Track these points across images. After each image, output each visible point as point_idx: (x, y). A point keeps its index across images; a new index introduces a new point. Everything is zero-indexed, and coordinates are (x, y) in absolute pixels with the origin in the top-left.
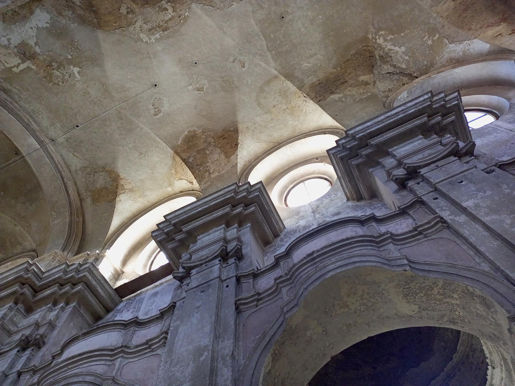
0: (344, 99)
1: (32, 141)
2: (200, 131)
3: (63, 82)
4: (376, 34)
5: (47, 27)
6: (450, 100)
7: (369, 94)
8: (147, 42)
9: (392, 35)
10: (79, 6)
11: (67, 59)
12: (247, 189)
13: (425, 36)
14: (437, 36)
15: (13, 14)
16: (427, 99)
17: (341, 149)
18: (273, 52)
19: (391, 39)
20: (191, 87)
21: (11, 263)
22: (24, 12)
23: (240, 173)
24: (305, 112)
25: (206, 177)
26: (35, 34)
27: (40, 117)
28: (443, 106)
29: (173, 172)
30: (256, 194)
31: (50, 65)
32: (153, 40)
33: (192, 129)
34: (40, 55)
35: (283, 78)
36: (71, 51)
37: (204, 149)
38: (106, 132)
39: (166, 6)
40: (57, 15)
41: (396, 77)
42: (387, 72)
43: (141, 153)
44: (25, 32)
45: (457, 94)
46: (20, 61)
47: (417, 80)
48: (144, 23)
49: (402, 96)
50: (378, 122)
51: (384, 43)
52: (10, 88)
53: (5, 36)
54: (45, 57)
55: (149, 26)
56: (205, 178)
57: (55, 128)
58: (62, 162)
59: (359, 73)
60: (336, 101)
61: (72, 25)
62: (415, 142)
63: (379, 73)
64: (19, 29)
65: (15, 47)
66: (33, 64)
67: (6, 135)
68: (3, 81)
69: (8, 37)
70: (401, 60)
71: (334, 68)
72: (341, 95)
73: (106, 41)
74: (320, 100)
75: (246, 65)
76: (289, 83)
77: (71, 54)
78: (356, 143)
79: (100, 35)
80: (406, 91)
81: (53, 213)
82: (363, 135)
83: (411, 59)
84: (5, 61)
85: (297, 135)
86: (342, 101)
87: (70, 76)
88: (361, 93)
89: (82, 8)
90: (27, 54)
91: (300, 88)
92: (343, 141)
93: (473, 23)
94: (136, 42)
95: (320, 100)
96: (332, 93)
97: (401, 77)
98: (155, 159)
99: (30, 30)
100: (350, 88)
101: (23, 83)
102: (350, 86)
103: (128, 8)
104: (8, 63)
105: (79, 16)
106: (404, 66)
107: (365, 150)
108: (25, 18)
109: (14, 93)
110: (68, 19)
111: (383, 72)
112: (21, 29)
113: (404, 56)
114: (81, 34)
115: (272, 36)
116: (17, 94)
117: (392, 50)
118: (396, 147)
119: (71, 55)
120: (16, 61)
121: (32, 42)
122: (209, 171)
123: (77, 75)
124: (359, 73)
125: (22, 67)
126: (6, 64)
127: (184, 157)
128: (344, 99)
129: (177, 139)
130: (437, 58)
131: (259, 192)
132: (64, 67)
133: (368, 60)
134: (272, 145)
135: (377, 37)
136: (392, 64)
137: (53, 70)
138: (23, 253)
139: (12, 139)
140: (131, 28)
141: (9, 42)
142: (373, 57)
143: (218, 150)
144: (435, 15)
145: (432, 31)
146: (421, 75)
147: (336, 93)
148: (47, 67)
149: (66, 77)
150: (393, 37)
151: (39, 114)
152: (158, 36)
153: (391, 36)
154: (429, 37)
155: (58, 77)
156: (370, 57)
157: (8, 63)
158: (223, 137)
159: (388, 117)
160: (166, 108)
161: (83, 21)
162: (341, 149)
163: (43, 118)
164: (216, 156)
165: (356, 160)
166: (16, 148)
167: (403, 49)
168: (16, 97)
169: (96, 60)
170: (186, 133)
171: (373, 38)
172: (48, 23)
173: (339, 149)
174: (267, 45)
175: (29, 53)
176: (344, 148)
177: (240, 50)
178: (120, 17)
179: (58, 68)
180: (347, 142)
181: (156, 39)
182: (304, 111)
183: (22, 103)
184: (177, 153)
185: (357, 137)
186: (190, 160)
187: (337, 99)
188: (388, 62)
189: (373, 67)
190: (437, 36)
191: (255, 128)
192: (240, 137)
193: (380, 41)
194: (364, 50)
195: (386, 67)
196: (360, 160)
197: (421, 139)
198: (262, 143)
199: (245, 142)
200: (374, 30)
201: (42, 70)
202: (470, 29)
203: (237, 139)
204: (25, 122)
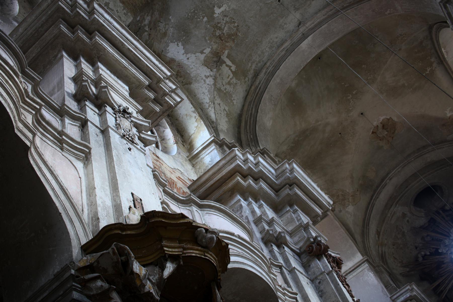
1: (304, 45)
3: (234, 22)
5: (183, 45)
10: (152, 17)
11: (208, 22)
15: (181, 77)
21: (443, 49)
26: (193, 55)
27: (276, 40)
31: (220, 37)
34: (212, 48)
36: (199, 18)
40: (167, 38)
44: (193, 64)
46: (224, 65)
52: (252, 72)
53: (205, 81)
54: (212, 43)
57: (285, 24)
58: (323, 12)
61: (172, 21)
64: (193, 70)
65: (211, 70)
66: (224, 53)
67: (302, 70)
68: (247, 79)
69: (204, 78)
77: (201, 18)
81: (388, 12)
84: (228, 78)
89: (153, 13)
90: (215, 59)
99: (190, 60)
101: (244, 60)
104: (229, 76)
108: (180, 65)
109: (256, 67)
110: (167, 26)
112: (192, 68)
116: (257, 64)
119: (203, 17)
120: (225, 69)
121: (202, 57)
123: (222, 9)
125: (229, 62)
126: (231, 77)
132: (218, 23)
137: (224, 34)
138: (432, 39)
139: (305, 64)
141: (209, 76)
148: (222, 40)
149: (228, 19)
151: (273, 41)
155: (229, 28)
157: (229, 76)
163: (277, 38)
166: (313, 59)
168: (259, 65)
172: (178, 44)
175: (213, 58)
179: (220, 29)
183: (265, 59)
201: (227, 44)
204: (285, 54)
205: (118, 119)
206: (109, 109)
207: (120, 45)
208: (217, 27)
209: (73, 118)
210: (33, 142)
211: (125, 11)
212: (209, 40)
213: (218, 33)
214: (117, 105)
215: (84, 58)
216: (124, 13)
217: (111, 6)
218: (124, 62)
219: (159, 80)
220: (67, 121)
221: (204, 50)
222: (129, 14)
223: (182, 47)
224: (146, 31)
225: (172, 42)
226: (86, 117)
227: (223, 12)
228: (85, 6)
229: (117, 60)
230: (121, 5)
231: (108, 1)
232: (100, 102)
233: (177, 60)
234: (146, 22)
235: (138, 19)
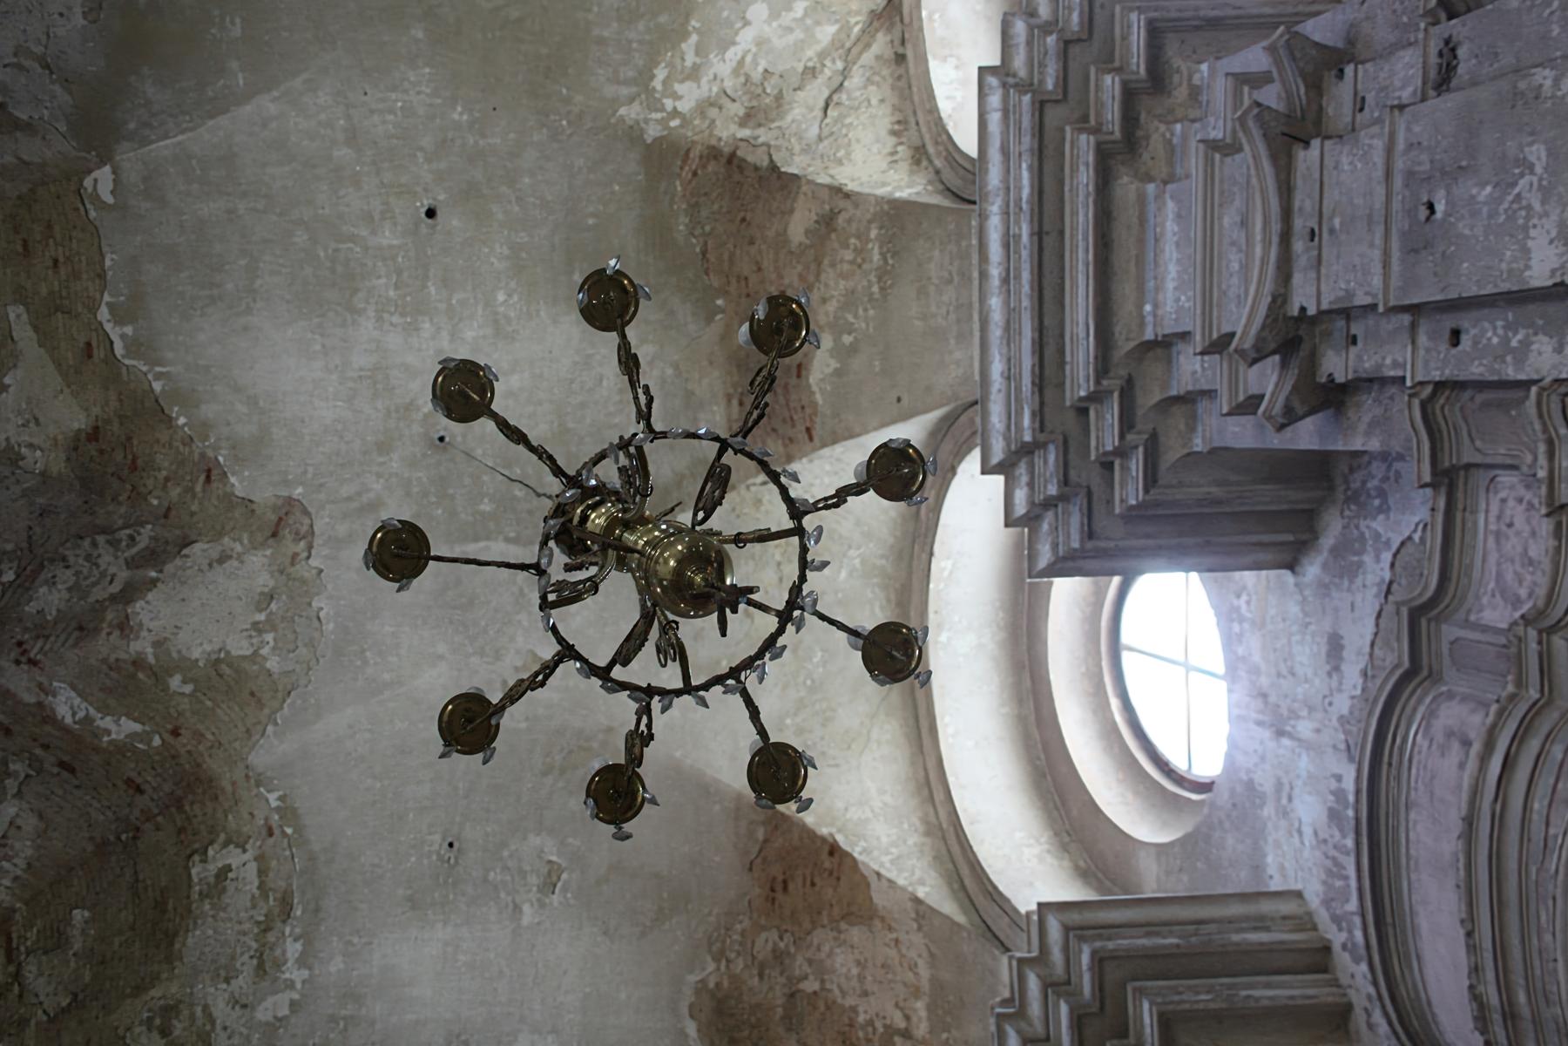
0: (847, 339)
50: (1007, 327)
59: (771, 233)
60: (838, 373)
63: (806, 150)
71: (709, 319)
74: (808, 430)
86: (853, 349)
88: (852, 262)
92: (1020, 496)
95: (808, 430)
102: (810, 288)
106: (827, 33)
115: (486, 507)
124: (771, 233)
128: (847, 339)
133: (737, 177)
174: (508, 540)
176: (1049, 504)
177: (481, 653)
180: (1031, 485)
187: (834, 364)
195: (796, 112)
198: (875, 735)
200: (636, 106)
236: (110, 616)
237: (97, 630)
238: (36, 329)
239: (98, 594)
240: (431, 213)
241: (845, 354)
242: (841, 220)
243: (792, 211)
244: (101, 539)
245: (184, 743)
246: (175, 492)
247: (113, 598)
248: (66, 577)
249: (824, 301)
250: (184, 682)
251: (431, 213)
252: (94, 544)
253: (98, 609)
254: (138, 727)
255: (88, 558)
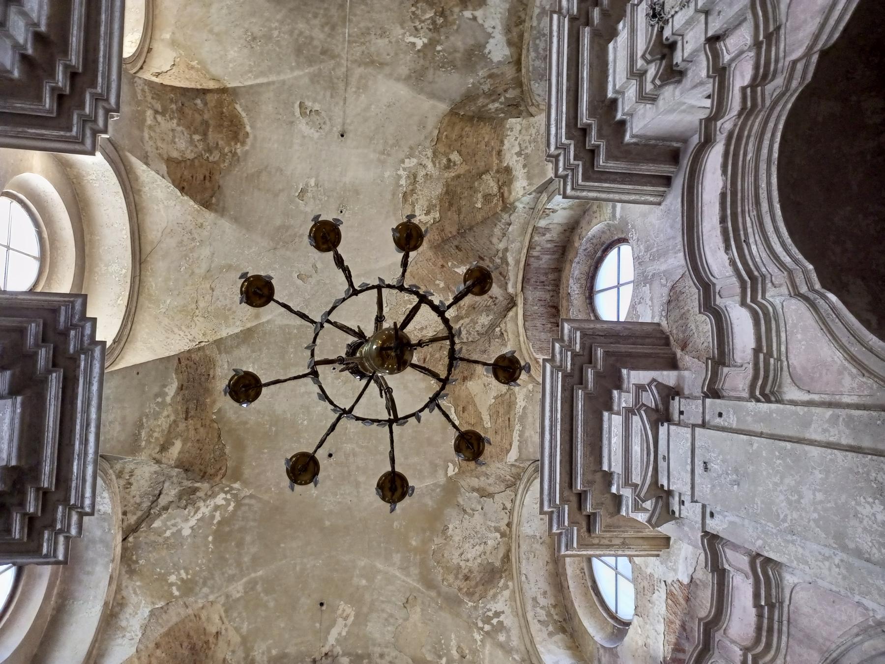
0: (159, 400)
2: (238, 151)
3: (413, 13)
4: (235, 496)
5: (485, 47)
6: (56, 543)
7: (143, 443)
8: (403, 162)
9: (219, 523)
10: (487, 105)
11: (439, 42)
12: (95, 121)
13: (187, 574)
14: (176, 593)
15: (520, 17)
16: (82, 502)
17: (75, 321)
18: (295, 331)
19: (213, 517)
20: (313, 184)
22: (515, 31)
23: (126, 156)
24: (172, 331)
25: (154, 102)
26: (486, 26)
28: (51, 525)
29: (194, 63)
30: (75, 129)
31: (442, 14)
32: (401, 172)
33: (249, 141)
35: (249, 325)
37: (205, 134)
38: (315, 16)
39: (432, 215)
41: (146, 505)
42: (164, 492)
43: (254, 39)
45: (61, 557)
47: (119, 538)
48: (427, 174)
49: (107, 500)
50: (89, 405)
51: (214, 504)
55: (420, 178)
56: (153, 98)
59: (189, 444)
60: (165, 386)
62: (10, 447)
70: (169, 523)
71: (220, 410)
72: (168, 399)
73: (434, 110)
75: (299, 282)
76: (237, 330)
78: (71, 351)
79: (443, 107)
80: (110, 511)
82: (79, 366)
83: (161, 540)
85: (141, 299)
86: (157, 396)
87: (416, 28)
88: (155, 431)
89: (483, 106)
91: (219, 343)
92: (88, 331)
93: (164, 655)
94: (411, 148)
96: (181, 388)
97: (139, 513)
98: (232, 52)
99: (493, 24)
100: (172, 418)
102: (175, 421)
103: (455, 164)
105: (477, 97)
107: (47, 359)
108: (508, 30)
110: (482, 81)
111: (167, 485)
112: (500, 13)
113: (174, 529)
114: (456, 83)
117: (196, 512)
118: (19, 411)
119: (439, 52)
121: (479, 13)
122: (163, 114)
123: (412, 39)
124: (189, 444)
127: (209, 97)
128: (159, 400)
129: (247, 109)
130: (138, 583)
131: (76, 138)
133: (202, 467)
134: (147, 248)
135: (229, 496)
136: (173, 505)
137: (435, 13)
140: (430, 153)
142: (203, 477)
143: (190, 155)
144: (211, 598)
145: (188, 588)
146: (124, 549)
147: (177, 393)
149: (417, 23)
150: (215, 522)
152: (403, 182)
153: (218, 516)
154: (182, 580)
155: (424, 12)
156: (205, 473)
158: (209, 177)
159: (88, 425)
160: (303, 126)
161: (469, 97)
162: (75, 321)
164: (182, 144)
165: (37, 334)
167: (186, 532)
169: (417, 79)
170: (248, 129)
171: (232, 489)
172: (489, 53)
173: (77, 317)
176: (74, 327)
177: (325, 284)
178: (450, 147)
179: (434, 22)
180: (83, 336)
181: (400, 177)
182: (176, 330)
184: (224, 90)
185: (83, 356)
186: (198, 101)
187: (166, 390)
188: (180, 499)
189: (186, 470)
190: (176, 593)
191: (193, 239)
192: (192, 203)
193: (220, 500)
194: (220, 469)
196: (30, 340)
197: (9, 460)
199: (178, 207)
202: (158, 646)
203: (192, 197)
205: (673, 13)
206: (667, 33)
207: (572, 93)
208: (435, 28)
209: (716, 55)
210: (808, 54)
211: (509, 133)
212: (455, 23)
213: (440, 21)
214: (653, 30)
215: (615, 117)
216: (512, 131)
217: (517, 149)
218: (585, 74)
219: (573, 19)
220: (727, 58)
221: (470, 19)
222: (508, 126)
223: (487, 45)
224: (505, 98)
225: (491, 61)
226: (705, 44)
227: (415, 37)
228: (561, 158)
229: (591, 81)
230: (506, 142)
231: (515, 156)
232: (666, 51)
233: (505, 38)
234: (497, 105)
235: (502, 115)
236: (464, 312)
237: (469, 307)
238: (481, 419)
239: (467, 320)
240: (330, 455)
241: (163, 394)
242: (158, 449)
243: (179, 453)
244: (465, 340)
245: (440, 262)
246: (437, 356)
247: (462, 318)
248: (478, 328)
249: (168, 416)
250: (438, 285)
251: (330, 455)
252: (467, 339)
253: (467, 315)
254: (456, 270)
255: (470, 334)
